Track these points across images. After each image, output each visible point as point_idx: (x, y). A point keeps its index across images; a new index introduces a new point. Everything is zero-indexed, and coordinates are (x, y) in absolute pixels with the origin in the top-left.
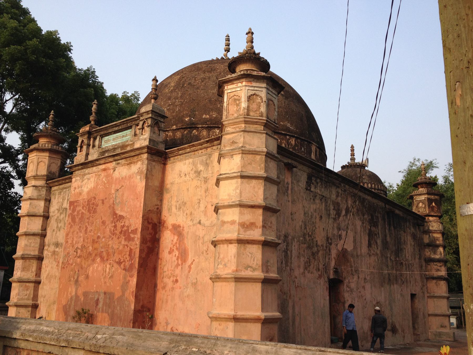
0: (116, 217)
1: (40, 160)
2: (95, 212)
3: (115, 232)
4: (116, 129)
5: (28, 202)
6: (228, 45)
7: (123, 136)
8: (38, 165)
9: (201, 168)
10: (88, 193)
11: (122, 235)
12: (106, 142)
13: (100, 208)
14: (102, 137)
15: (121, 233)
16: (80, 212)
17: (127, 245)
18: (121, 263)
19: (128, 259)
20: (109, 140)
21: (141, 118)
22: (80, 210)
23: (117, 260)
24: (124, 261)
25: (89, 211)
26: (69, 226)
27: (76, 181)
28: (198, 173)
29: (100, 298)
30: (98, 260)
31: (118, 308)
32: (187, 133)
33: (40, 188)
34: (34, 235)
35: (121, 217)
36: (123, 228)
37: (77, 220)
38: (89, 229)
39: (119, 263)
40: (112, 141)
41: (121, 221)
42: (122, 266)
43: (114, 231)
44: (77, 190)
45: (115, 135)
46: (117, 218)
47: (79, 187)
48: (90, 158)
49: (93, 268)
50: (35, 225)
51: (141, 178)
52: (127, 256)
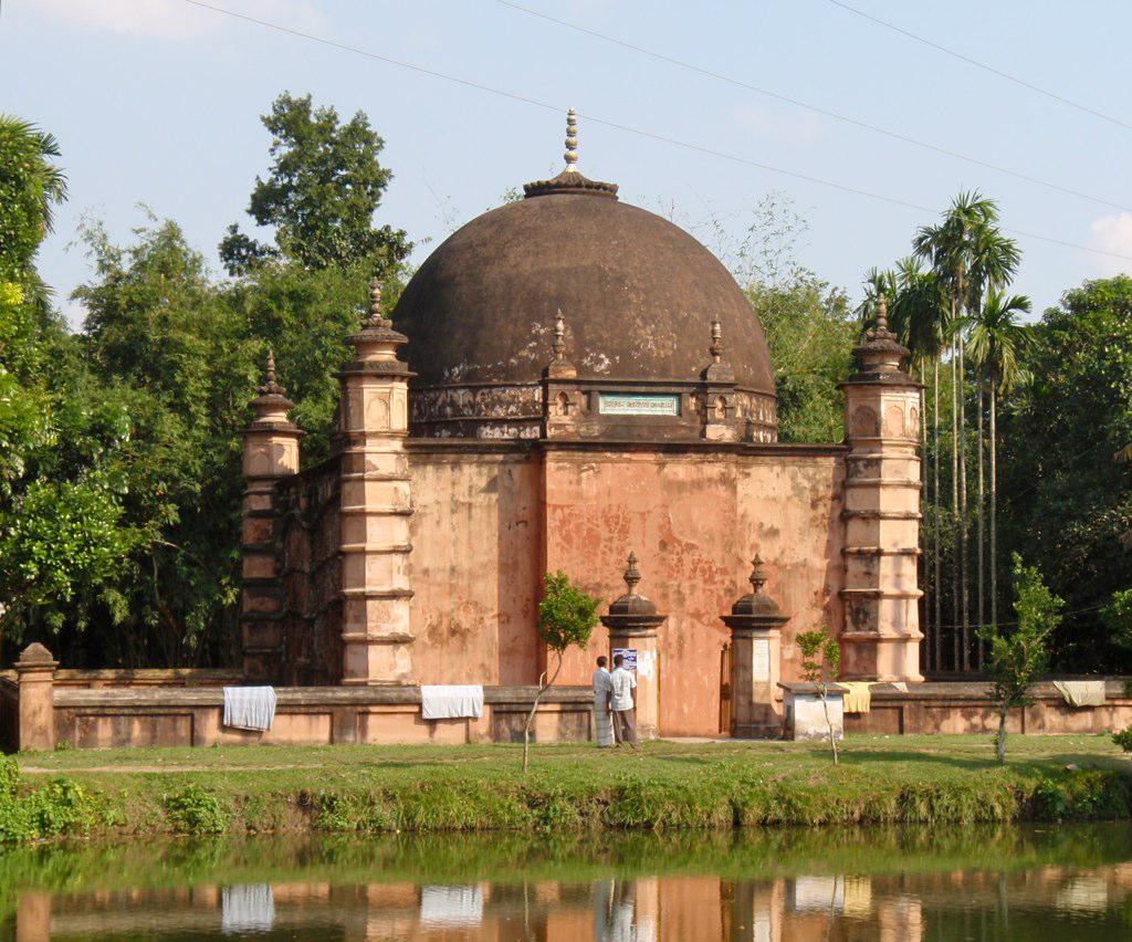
0: (680, 545)
2: (624, 531)
4: (643, 389)
6: (570, 133)
13: (635, 525)
14: (603, 393)
15: (694, 570)
16: (585, 527)
20: (620, 405)
22: (582, 523)
23: (691, 611)
24: (708, 613)
26: (559, 549)
27: (559, 469)
31: (705, 678)
35: (691, 547)
37: (576, 540)
39: (697, 615)
42: (705, 619)
43: (677, 566)
44: (566, 487)
51: (726, 490)
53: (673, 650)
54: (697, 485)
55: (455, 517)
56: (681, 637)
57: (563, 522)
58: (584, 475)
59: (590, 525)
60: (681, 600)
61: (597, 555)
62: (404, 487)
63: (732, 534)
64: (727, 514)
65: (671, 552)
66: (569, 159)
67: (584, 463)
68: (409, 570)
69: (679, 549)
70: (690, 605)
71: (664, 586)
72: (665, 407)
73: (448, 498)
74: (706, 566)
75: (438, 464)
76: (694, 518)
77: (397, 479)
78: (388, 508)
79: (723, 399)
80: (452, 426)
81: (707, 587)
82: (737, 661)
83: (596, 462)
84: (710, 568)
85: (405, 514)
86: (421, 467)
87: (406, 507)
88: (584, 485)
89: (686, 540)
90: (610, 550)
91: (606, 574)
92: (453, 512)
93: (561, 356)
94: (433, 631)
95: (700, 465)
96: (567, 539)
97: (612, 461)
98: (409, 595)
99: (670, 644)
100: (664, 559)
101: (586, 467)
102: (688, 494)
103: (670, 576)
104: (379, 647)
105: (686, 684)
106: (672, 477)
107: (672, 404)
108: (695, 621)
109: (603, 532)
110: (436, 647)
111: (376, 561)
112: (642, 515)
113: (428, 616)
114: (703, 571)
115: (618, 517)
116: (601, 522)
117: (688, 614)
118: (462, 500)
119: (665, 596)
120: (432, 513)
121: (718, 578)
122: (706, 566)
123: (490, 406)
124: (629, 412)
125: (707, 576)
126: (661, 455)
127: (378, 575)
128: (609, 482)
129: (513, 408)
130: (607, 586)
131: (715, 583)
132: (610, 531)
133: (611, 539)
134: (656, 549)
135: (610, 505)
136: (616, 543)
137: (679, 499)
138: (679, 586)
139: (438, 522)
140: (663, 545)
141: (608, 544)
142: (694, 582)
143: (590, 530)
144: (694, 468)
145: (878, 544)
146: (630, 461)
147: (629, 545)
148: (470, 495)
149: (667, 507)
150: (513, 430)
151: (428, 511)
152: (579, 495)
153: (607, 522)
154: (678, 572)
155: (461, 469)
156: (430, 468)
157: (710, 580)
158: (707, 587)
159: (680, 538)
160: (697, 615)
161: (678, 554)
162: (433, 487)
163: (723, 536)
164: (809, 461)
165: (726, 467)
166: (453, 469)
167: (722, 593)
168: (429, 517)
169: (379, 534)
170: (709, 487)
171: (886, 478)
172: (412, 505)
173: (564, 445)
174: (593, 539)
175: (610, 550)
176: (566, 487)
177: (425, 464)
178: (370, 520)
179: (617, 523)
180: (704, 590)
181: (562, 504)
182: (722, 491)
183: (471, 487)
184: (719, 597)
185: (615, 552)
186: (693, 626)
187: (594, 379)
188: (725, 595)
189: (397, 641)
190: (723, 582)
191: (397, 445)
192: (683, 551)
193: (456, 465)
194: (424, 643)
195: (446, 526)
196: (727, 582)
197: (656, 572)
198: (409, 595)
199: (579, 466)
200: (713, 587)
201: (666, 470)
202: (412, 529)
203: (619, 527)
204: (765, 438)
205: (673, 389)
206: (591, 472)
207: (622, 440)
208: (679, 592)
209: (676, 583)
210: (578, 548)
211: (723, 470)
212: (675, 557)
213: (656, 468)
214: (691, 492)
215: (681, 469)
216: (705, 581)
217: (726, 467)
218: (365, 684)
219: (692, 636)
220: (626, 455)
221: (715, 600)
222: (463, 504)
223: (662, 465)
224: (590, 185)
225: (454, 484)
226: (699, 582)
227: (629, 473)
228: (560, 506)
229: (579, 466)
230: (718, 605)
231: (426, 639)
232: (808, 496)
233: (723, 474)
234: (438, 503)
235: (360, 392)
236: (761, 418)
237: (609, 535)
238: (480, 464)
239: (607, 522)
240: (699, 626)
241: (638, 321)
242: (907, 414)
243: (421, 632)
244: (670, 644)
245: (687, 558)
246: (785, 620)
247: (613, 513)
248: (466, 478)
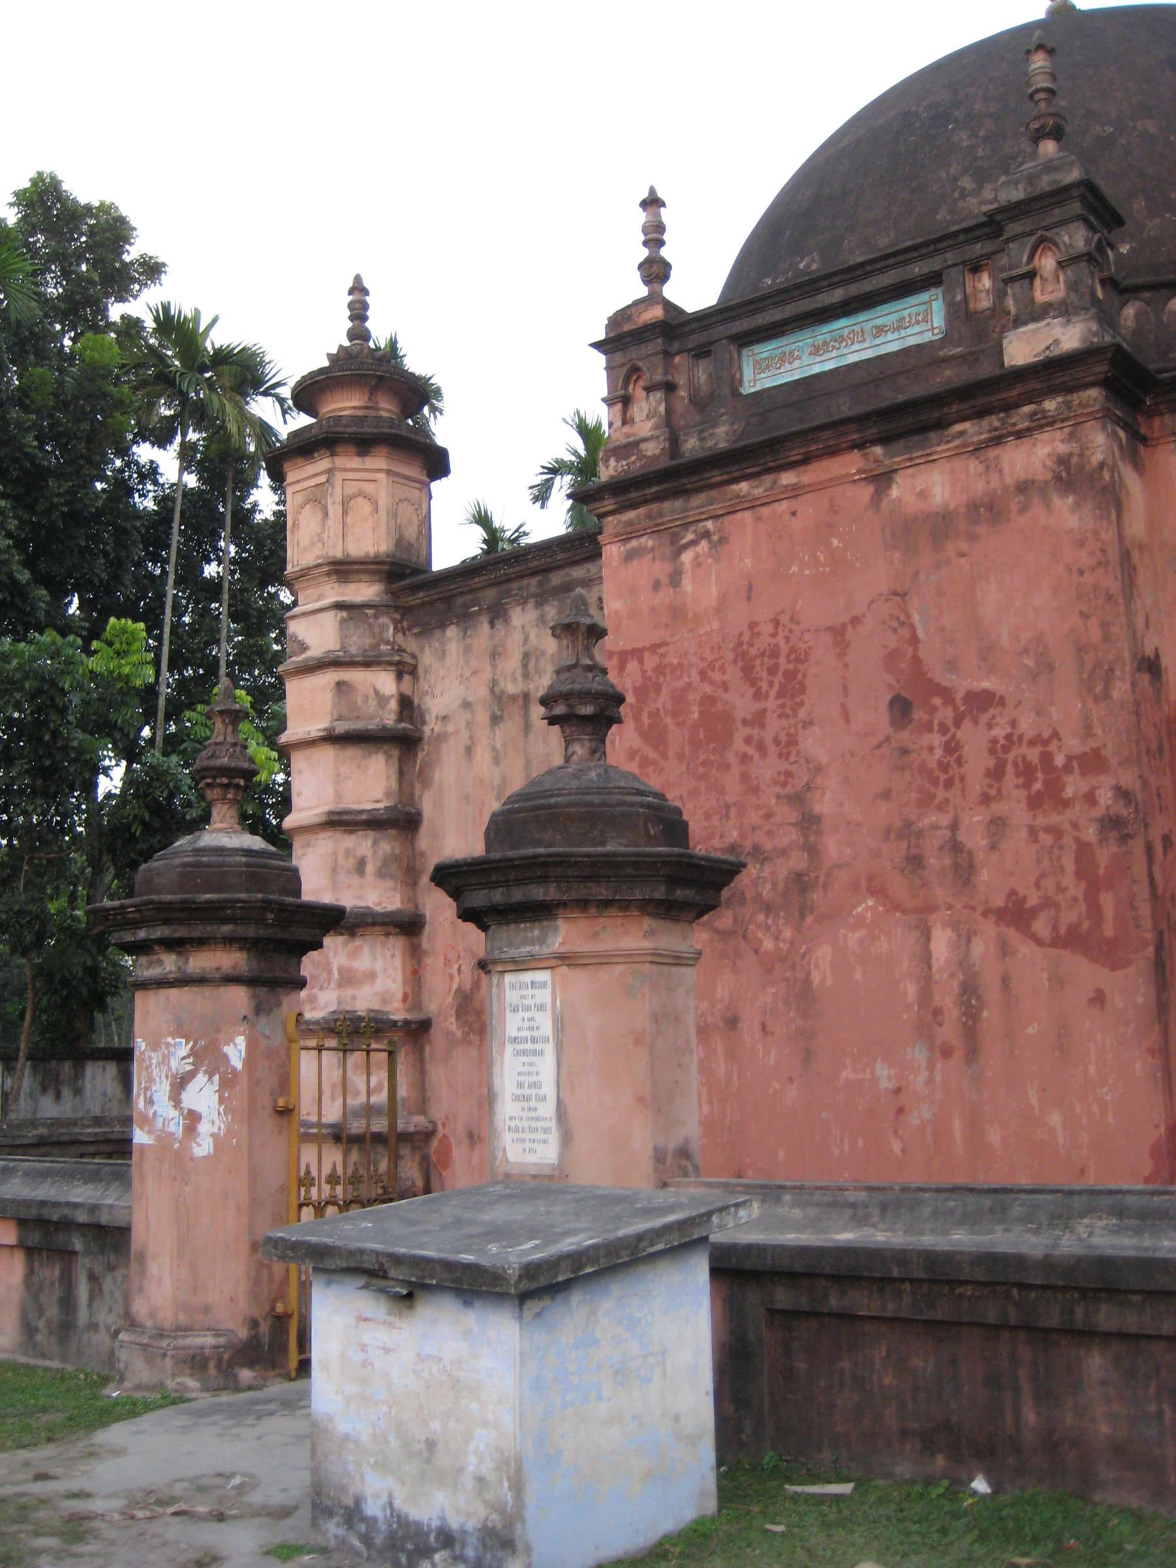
1: (352, 488)
2: (792, 688)
3: (955, 770)
4: (838, 295)
5: (328, 678)
7: (880, 330)
8: (345, 512)
12: (761, 366)
15: (996, 774)
16: (694, 697)
17: (1048, 830)
18: (1034, 912)
19: (1075, 888)
21: (1013, 228)
22: (689, 686)
23: (999, 902)
24: (1048, 903)
27: (629, 557)
31: (1055, 1119)
32: (1138, 316)
33: (370, 612)
34: (373, 823)
35: (982, 701)
36: (1006, 749)
37: (676, 737)
39: (1016, 914)
40: (807, 359)
41: (984, 718)
42: (1041, 926)
43: (943, 767)
44: (646, 599)
45: (826, 328)
48: (691, 445)
50: (370, 782)
52: (1068, 880)
53: (948, 1032)
54: (988, 511)
55: (500, 731)
56: (970, 989)
58: (687, 557)
59: (707, 688)
60: (963, 871)
61: (727, 767)
62: (386, 682)
63: (1106, 639)
64: (1087, 578)
65: (928, 727)
67: (686, 526)
69: (946, 714)
70: (991, 882)
71: (907, 831)
72: (910, 325)
73: (483, 692)
74: (1033, 755)
75: (466, 619)
81: (1041, 821)
83: (715, 517)
84: (1047, 758)
86: (437, 633)
87: (389, 717)
88: (687, 585)
89: (962, 684)
90: (761, 748)
91: (753, 817)
92: (495, 720)
95: (992, 453)
97: (753, 505)
99: (937, 1012)
100: (905, 752)
101: (690, 536)
102: (964, 546)
103: (926, 801)
105: (994, 1137)
107: (927, 317)
108: (1012, 933)
109: (742, 704)
110: (469, 1043)
111: (309, 850)
112: (838, 633)
113: (454, 971)
114: (1026, 772)
115: (775, 653)
116: (733, 674)
117: (985, 914)
118: (511, 689)
119: (915, 861)
120: (456, 732)
121: (1073, 785)
122: (1033, 755)
124: (817, 369)
125: (1038, 786)
126: (878, 450)
128: (748, 562)
130: (756, 849)
131: (1066, 804)
132: (758, 696)
133: (759, 719)
134: (879, 718)
135: (753, 625)
136: (774, 725)
137: (938, 566)
138: (954, 826)
139: (469, 751)
140: (901, 708)
141: (756, 732)
142: (999, 808)
143: (708, 701)
144: (974, 466)
146: (795, 492)
147: (808, 724)
148: (526, 676)
149: (904, 595)
151: (450, 728)
152: (677, 613)
153: (747, 671)
154: (949, 784)
155: (507, 622)
156: (452, 632)
157: (1049, 797)
158: (1041, 821)
159: (948, 679)
160: (1016, 914)
161: (943, 729)
163: (1081, 649)
165: (1072, 436)
166: (492, 624)
167: (1090, 834)
168: (452, 741)
170: (1024, 509)
174: (715, 726)
175: (761, 748)
176: (646, 599)
179: (772, 671)
180: (1033, 832)
181: (638, 645)
182: (1067, 514)
183: (526, 655)
184: (1083, 850)
185: (772, 749)
186: (1005, 950)
188: (1103, 840)
190: (1090, 798)
192: (958, 721)
193: (497, 613)
194: (449, 1034)
195: (482, 755)
196: (1105, 797)
197: (886, 795)
199: (675, 538)
200: (1055, 819)
201: (895, 492)
203: (779, 678)
206: (704, 545)
208: (956, 847)
209: (944, 820)
210: (681, 757)
211: (1062, 448)
212: (937, 739)
213: (866, 492)
214: (972, 538)
215: (934, 482)
216: (1035, 803)
217: (1072, 436)
219: (1005, 981)
220: (787, 478)
221: (1069, 864)
222: (513, 698)
223: (881, 479)
225: (495, 655)
226: (1014, 805)
227: (797, 524)
228: (634, 651)
230: (1080, 874)
231: (452, 1024)
233: (1063, 461)
234: (466, 705)
237: (758, 706)
238: (541, 599)
239: (748, 672)
240: (1025, 949)
241: (966, 183)
244: (937, 1012)
245: (974, 739)
247: (763, 643)
248: (517, 637)
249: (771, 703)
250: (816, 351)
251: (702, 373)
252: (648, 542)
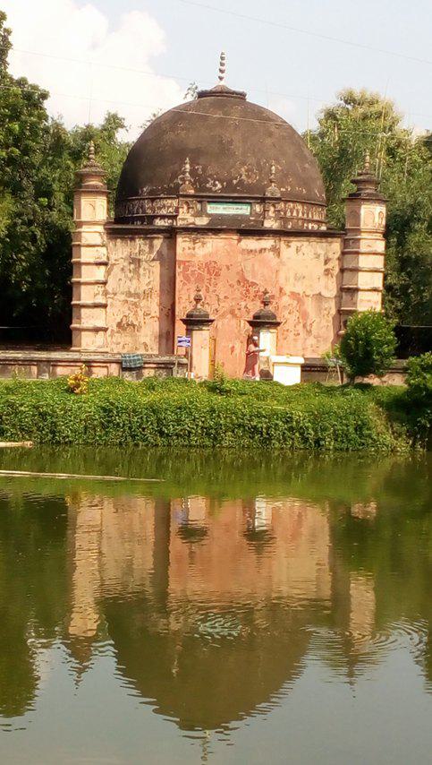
2: (217, 275)
4: (231, 200)
6: (222, 64)
9: (322, 252)
10: (205, 256)
11: (257, 298)
13: (224, 272)
14: (209, 202)
25: (209, 272)
28: (318, 256)
29: (236, 346)
30: (229, 316)
37: (192, 279)
38: (211, 289)
44: (187, 251)
46: (242, 281)
47: (189, 249)
49: (223, 324)
57: (186, 269)
66: (221, 78)
68: (106, 293)
72: (244, 210)
76: (256, 269)
77: (98, 246)
78: (92, 261)
79: (275, 207)
80: (142, 219)
82: (251, 340)
85: (105, 264)
87: (104, 259)
93: (187, 183)
94: (119, 325)
96: (187, 278)
98: (105, 306)
104: (87, 333)
106: (244, 247)
123: (160, 208)
127: (86, 295)
129: (170, 209)
145: (356, 284)
150: (170, 221)
152: (194, 255)
156: (119, 240)
162: (121, 251)
164: (324, 240)
169: (87, 274)
171: (363, 249)
172: (108, 258)
173: (188, 230)
177: (116, 238)
178: (83, 267)
187: (211, 194)
189: (96, 330)
191: (100, 229)
193: (132, 239)
198: (105, 306)
202: (108, 273)
204: (313, 227)
205: (248, 201)
207: (214, 229)
215: (251, 243)
218: (79, 351)
223: (239, 241)
224: (234, 93)
229: (194, 241)
232: (322, 259)
235: (80, 201)
236: (310, 216)
238: (145, 239)
242: (377, 216)
243: (113, 326)
245: (252, 290)
246: (278, 324)
249: (213, 276)
250: (224, 208)
251: (199, 206)
252: (187, 239)
